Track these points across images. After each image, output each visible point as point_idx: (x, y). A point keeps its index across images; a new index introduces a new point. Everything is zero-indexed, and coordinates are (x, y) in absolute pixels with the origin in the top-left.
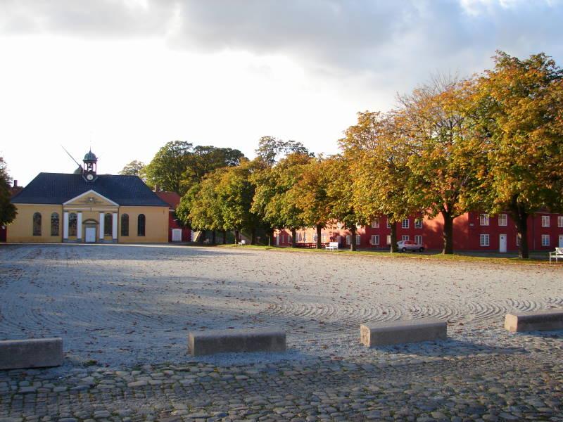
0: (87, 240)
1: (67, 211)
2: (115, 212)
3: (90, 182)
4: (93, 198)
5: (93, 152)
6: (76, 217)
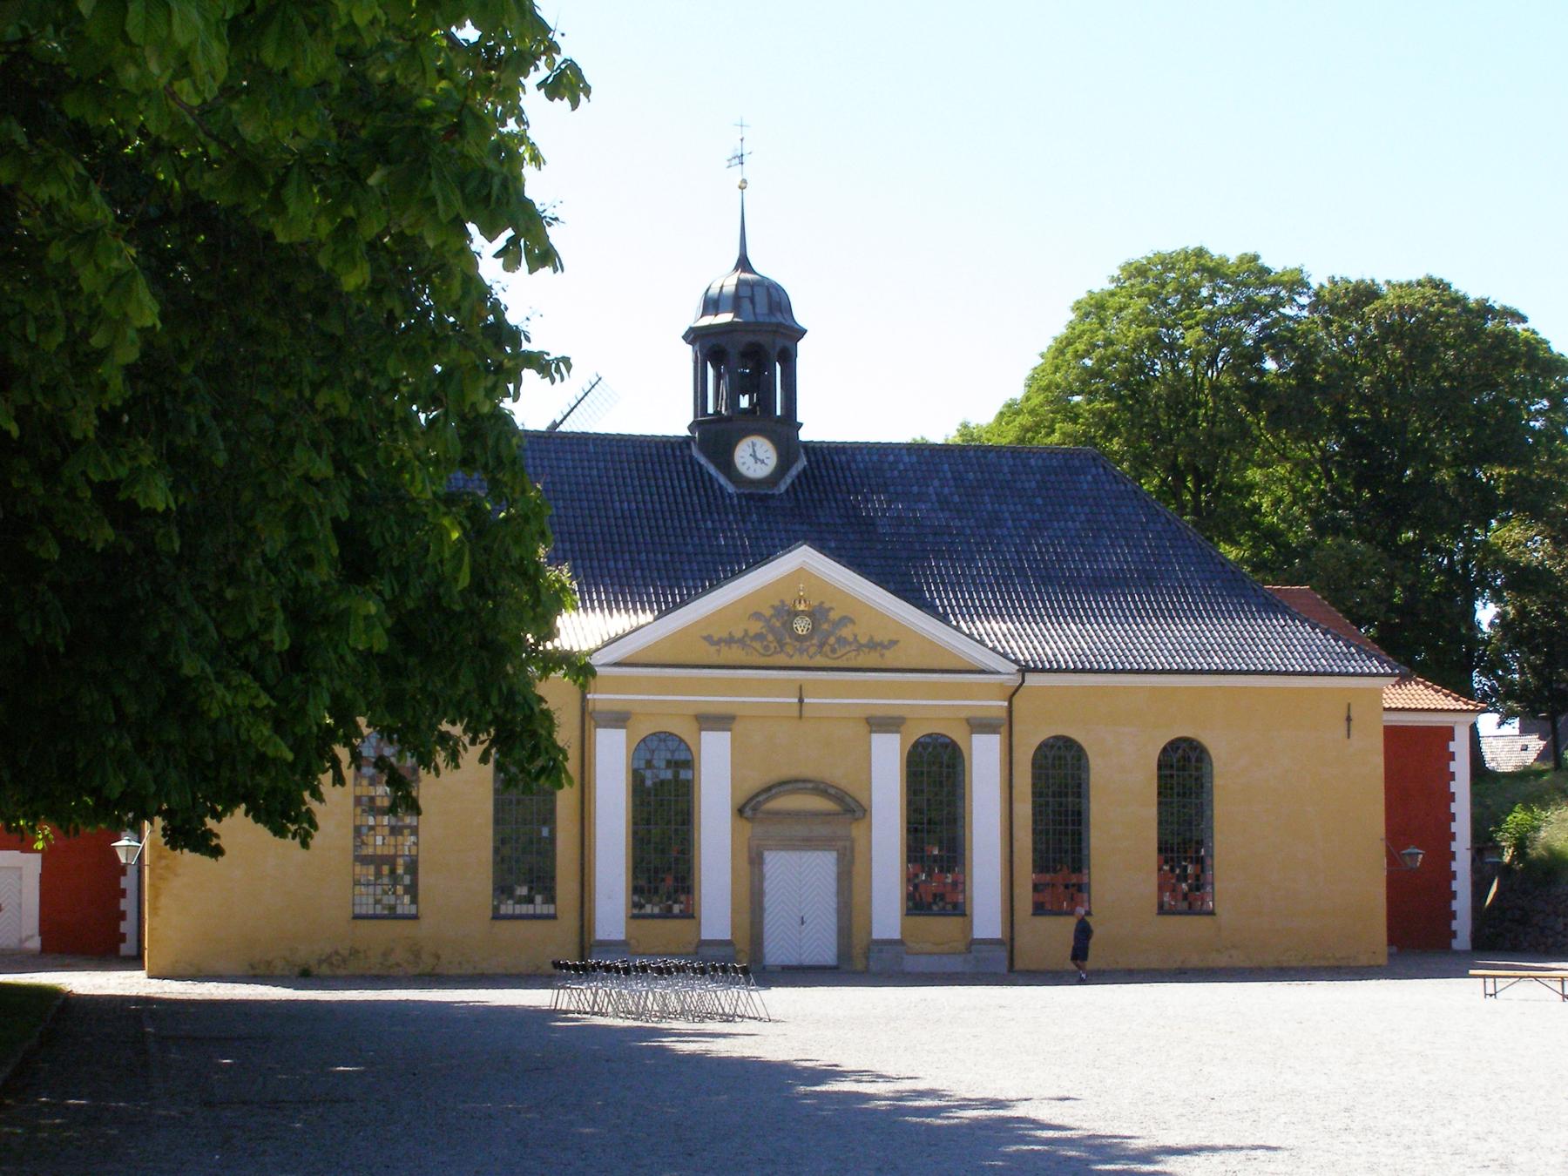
0: (775, 953)
1: (619, 719)
2: (981, 725)
3: (756, 495)
4: (817, 615)
5: (765, 266)
6: (689, 764)
